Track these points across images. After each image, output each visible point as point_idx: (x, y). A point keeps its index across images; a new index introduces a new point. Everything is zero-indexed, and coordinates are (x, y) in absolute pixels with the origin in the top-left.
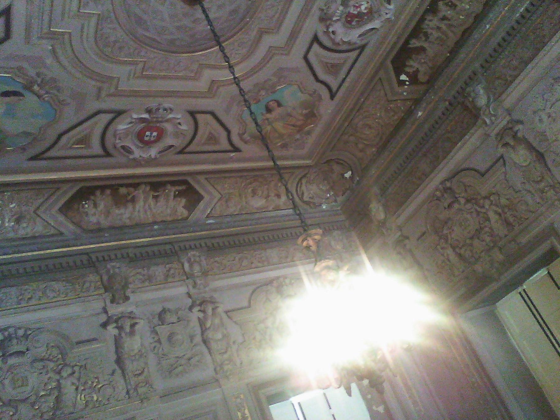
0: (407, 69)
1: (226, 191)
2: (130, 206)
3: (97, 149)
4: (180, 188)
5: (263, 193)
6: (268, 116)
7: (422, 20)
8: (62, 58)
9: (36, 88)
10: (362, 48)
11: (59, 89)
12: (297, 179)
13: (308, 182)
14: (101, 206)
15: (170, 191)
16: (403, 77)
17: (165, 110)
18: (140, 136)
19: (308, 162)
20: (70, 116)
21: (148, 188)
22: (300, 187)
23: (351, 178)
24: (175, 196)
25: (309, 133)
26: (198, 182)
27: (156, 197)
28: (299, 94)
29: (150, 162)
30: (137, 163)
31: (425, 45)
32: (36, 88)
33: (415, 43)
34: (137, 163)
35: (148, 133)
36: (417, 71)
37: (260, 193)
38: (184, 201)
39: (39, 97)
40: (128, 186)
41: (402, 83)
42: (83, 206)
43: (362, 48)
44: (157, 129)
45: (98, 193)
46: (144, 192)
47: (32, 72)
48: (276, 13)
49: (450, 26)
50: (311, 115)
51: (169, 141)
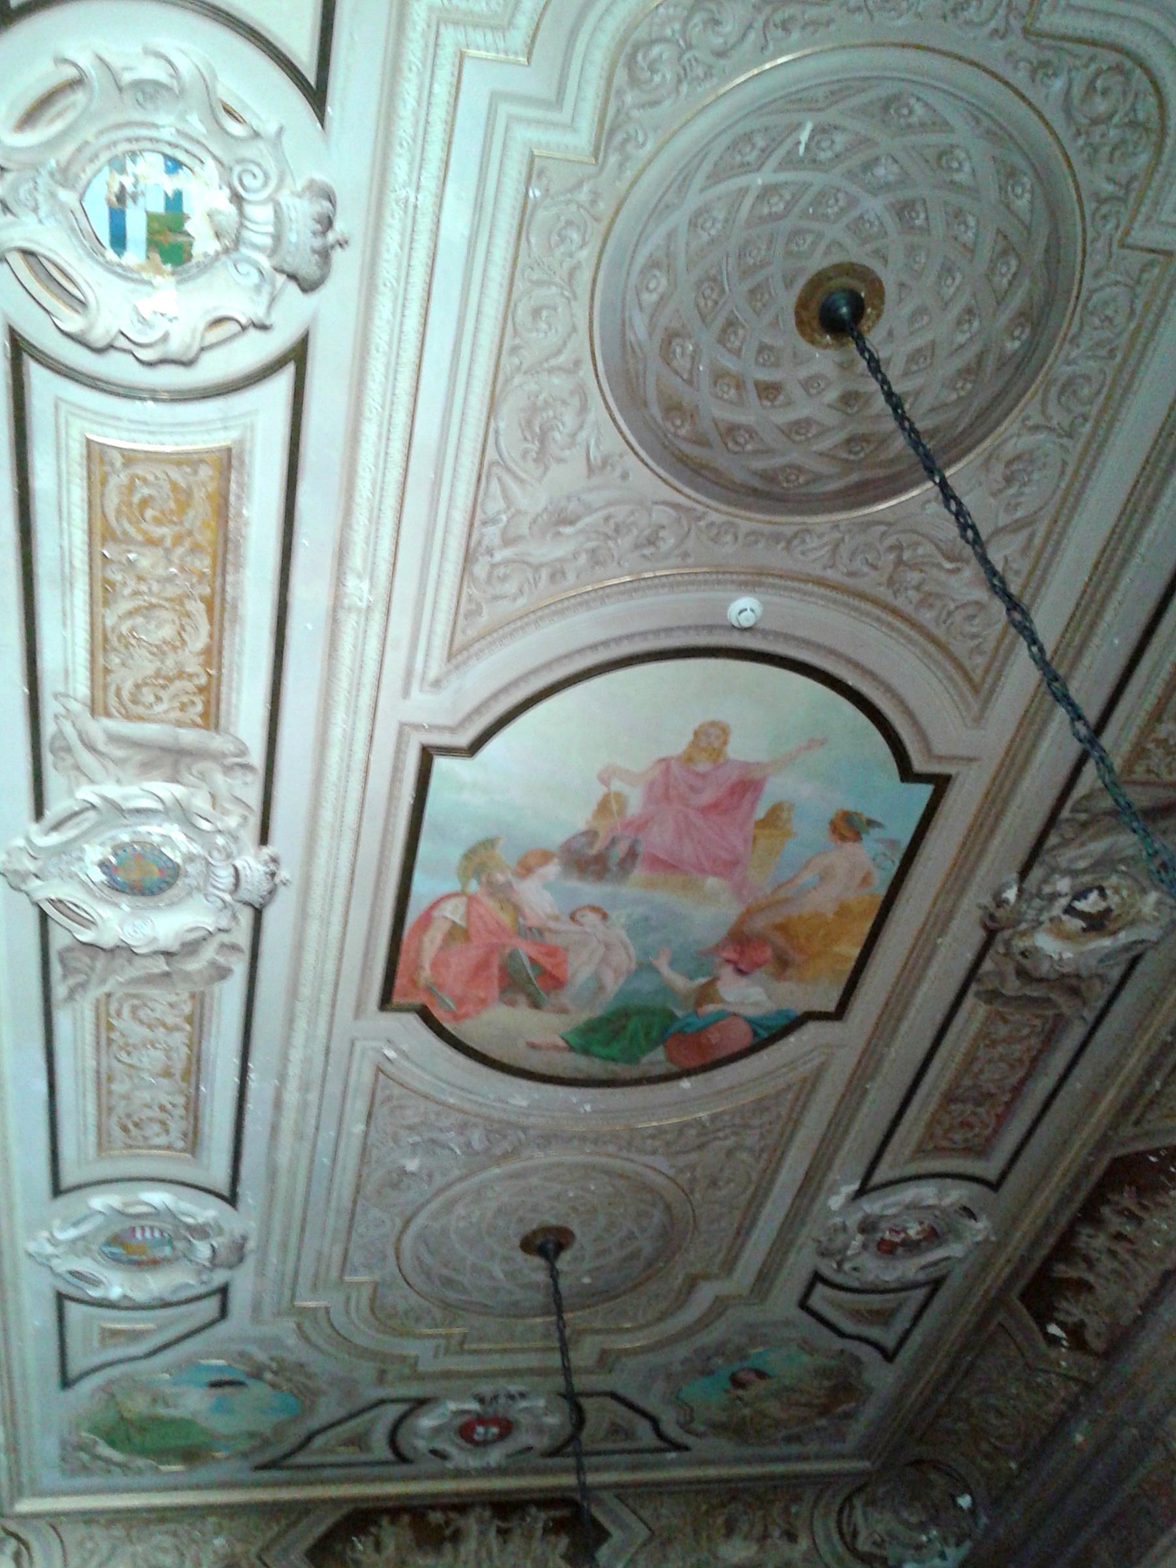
0: (1061, 1317)
1: (664, 1522)
2: (448, 1547)
3: (380, 1449)
4: (557, 1513)
5: (752, 1526)
6: (740, 1392)
7: (1069, 1235)
8: (314, 1337)
9: (268, 1376)
10: (936, 1285)
11: (309, 1376)
12: (839, 1500)
13: (871, 1503)
14: (390, 1548)
15: (535, 1519)
16: (1054, 1329)
17: (511, 1397)
18: (465, 1432)
19: (865, 1465)
20: (327, 1409)
21: (487, 1514)
22: (850, 1516)
23: (973, 1511)
24: (546, 1531)
25: (847, 1416)
26: (600, 1502)
27: (503, 1533)
28: (805, 1358)
29: (487, 1472)
30: (459, 1474)
31: (1091, 1278)
32: (268, 1376)
33: (1062, 1270)
34: (459, 1474)
35: (480, 1429)
36: (1082, 1325)
37: (745, 1528)
38: (563, 1542)
39: (273, 1386)
40: (445, 1508)
41: (1053, 1341)
42: (353, 1547)
43: (936, 1285)
44: (496, 1421)
45: (385, 1521)
46: (480, 1521)
47: (261, 1356)
48: (719, 1250)
49: (1136, 1254)
50: (843, 1387)
51: (523, 1438)
